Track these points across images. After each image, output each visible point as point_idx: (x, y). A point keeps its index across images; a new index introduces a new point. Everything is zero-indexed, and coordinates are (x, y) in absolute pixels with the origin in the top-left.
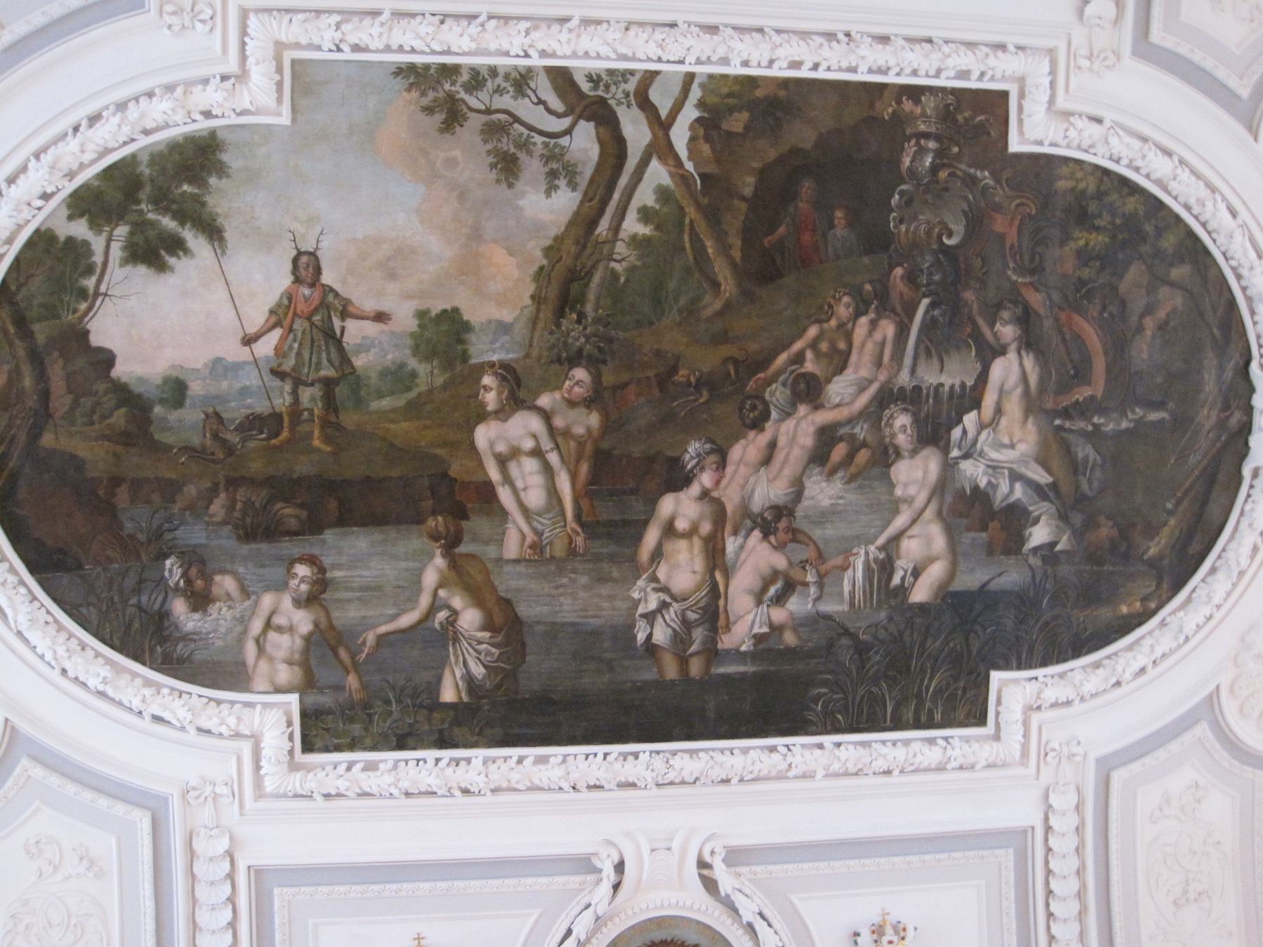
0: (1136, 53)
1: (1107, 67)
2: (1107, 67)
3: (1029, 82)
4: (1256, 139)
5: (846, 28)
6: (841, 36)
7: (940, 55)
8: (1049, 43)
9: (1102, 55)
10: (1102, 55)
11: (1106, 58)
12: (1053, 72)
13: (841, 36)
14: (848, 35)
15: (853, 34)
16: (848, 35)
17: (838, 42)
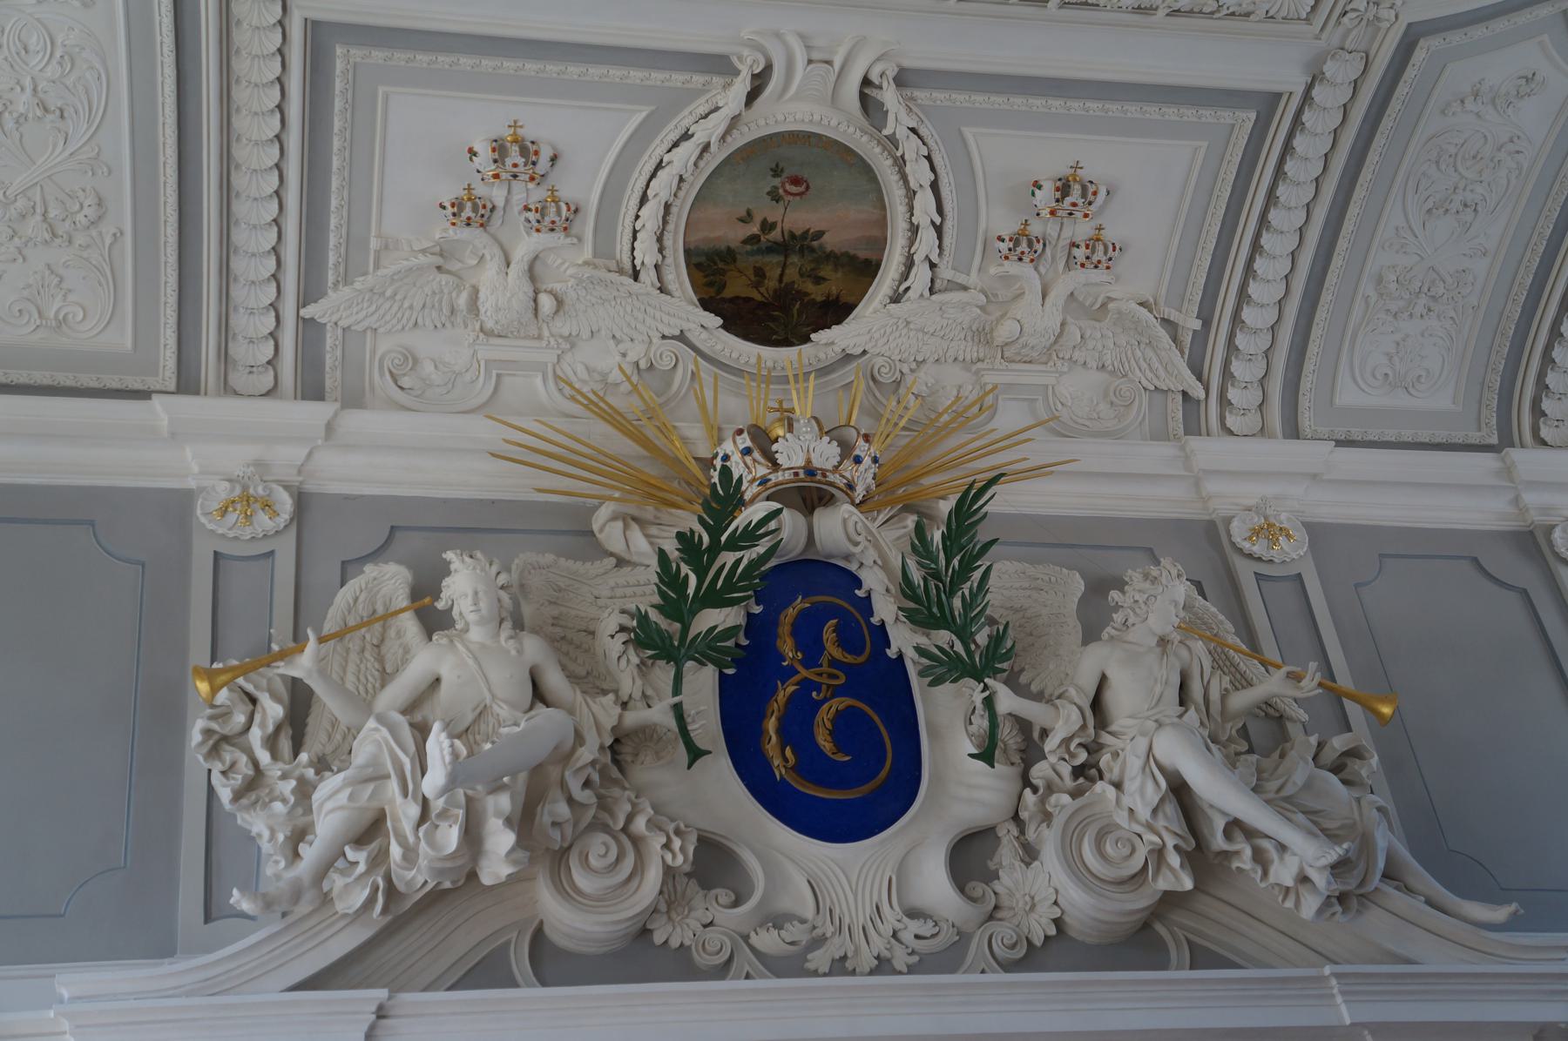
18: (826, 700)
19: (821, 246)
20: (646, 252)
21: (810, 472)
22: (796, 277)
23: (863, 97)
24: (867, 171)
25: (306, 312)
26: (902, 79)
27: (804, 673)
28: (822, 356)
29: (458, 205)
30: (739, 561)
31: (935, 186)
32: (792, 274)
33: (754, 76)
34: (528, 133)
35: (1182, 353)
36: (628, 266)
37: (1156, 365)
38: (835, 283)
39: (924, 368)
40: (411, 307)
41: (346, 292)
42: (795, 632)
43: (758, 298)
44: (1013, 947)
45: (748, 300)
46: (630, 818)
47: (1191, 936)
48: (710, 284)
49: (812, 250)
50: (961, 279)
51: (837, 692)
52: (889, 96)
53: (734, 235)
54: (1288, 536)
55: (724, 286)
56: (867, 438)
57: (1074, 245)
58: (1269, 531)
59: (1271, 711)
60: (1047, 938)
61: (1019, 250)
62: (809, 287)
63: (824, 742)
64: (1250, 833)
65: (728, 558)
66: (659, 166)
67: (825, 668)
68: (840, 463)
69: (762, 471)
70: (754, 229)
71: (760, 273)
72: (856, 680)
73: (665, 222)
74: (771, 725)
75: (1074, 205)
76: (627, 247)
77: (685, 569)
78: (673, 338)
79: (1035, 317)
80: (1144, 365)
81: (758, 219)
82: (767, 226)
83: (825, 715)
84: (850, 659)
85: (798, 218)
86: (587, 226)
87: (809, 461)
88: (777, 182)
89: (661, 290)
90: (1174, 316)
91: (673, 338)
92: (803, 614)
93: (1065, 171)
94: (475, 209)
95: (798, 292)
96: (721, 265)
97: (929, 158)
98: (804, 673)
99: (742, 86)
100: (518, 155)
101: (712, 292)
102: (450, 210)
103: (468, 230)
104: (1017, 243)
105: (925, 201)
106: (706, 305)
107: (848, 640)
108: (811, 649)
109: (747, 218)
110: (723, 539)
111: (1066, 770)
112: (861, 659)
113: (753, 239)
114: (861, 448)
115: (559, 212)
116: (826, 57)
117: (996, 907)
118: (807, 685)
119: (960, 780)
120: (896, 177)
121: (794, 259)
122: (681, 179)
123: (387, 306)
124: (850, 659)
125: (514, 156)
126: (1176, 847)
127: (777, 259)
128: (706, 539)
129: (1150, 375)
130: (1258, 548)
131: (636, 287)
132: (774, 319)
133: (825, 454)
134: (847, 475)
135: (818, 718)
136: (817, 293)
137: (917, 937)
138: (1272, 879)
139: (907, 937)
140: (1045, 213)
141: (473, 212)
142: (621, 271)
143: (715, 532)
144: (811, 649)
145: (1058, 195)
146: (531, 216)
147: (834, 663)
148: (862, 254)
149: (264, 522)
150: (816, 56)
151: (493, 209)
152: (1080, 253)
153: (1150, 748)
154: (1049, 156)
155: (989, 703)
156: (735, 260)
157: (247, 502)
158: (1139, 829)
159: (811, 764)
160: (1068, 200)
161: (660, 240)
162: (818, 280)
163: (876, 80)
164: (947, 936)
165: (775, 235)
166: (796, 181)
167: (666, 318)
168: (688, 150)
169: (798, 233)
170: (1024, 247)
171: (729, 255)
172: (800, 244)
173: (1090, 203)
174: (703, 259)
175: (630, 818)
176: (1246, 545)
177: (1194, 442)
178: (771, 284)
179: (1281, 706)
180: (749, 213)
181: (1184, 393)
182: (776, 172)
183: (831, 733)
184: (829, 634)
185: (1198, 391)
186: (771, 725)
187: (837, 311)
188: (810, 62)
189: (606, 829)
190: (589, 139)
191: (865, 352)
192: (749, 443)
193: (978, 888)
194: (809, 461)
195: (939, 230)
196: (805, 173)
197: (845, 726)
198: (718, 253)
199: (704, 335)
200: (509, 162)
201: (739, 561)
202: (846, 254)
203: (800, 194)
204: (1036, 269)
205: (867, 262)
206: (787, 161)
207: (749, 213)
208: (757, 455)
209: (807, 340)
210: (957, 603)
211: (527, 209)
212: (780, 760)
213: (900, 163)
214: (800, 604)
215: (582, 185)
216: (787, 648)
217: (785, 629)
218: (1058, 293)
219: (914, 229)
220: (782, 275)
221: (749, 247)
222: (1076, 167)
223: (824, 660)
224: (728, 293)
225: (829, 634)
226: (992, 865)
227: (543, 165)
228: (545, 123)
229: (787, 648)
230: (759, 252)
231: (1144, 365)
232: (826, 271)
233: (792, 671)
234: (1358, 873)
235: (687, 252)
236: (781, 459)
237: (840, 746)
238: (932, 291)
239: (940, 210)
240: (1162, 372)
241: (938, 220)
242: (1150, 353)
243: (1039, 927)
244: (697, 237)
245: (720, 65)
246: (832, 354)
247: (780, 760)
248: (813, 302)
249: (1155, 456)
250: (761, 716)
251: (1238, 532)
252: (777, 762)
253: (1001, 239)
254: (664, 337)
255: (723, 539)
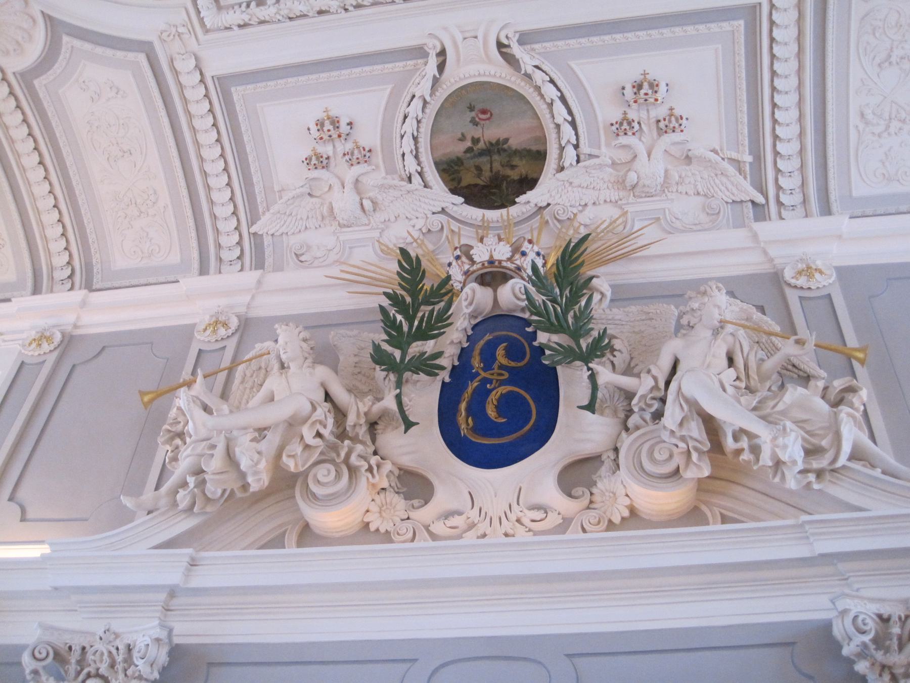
0: (150, 44)
1: (165, 31)
2: (165, 31)
3: (215, 9)
4: (42, 12)
5: (348, 14)
6: (351, 8)
7: (282, 13)
8: (211, 36)
9: (172, 37)
10: (172, 37)
11: (169, 36)
12: (201, 21)
13: (351, 8)
14: (346, 10)
15: (343, 11)
16: (346, 10)
17: (352, 5)
18: (493, 389)
19: (509, 147)
20: (411, 165)
21: (491, 262)
22: (500, 168)
23: (501, 53)
24: (522, 98)
25: (252, 230)
26: (525, 39)
27: (483, 374)
28: (524, 210)
29: (308, 160)
30: (432, 311)
31: (563, 99)
32: (497, 166)
33: (438, 55)
34: (333, 113)
35: (745, 178)
36: (405, 177)
37: (730, 187)
38: (523, 168)
39: (588, 209)
40: (301, 219)
41: (268, 215)
42: (481, 353)
43: (481, 183)
44: (599, 523)
45: (476, 185)
46: (348, 455)
47: (723, 511)
48: (453, 180)
49: (505, 150)
50: (595, 152)
51: (502, 383)
52: (516, 50)
53: (458, 149)
54: (821, 272)
55: (460, 181)
56: (530, 242)
57: (659, 121)
58: (808, 271)
59: (801, 373)
60: (623, 519)
61: (623, 128)
62: (509, 172)
63: (491, 412)
64: (751, 436)
65: (425, 309)
66: (405, 117)
67: (496, 370)
68: (512, 256)
69: (466, 267)
70: (469, 144)
71: (479, 169)
72: (515, 376)
73: (417, 149)
74: (463, 406)
75: (646, 94)
76: (401, 166)
77: (399, 317)
78: (439, 213)
79: (651, 170)
80: (723, 188)
81: (469, 137)
82: (475, 141)
83: (494, 397)
84: (513, 364)
85: (491, 133)
86: (378, 158)
87: (491, 256)
88: (473, 114)
89: (425, 186)
90: (734, 155)
91: (439, 213)
92: (488, 343)
93: (639, 78)
94: (317, 159)
95: (503, 176)
96: (456, 168)
97: (552, 81)
98: (483, 374)
99: (433, 62)
100: (331, 127)
101: (455, 184)
102: (306, 162)
103: (316, 171)
104: (621, 124)
105: (559, 107)
106: (454, 191)
107: (514, 351)
108: (488, 358)
109: (463, 138)
110: (420, 297)
111: (648, 417)
112: (519, 364)
113: (469, 150)
114: (526, 247)
115: (360, 152)
116: (473, 34)
117: (591, 502)
118: (485, 381)
119: (578, 429)
120: (538, 98)
121: (496, 157)
122: (419, 122)
123: (289, 220)
124: (513, 364)
125: (328, 126)
126: (696, 449)
127: (485, 159)
128: (408, 299)
129: (728, 193)
130: (802, 281)
131: (410, 187)
132: (494, 194)
133: (502, 252)
134: (518, 262)
135: (489, 399)
136: (514, 175)
137: (533, 521)
138: (761, 463)
139: (526, 521)
140: (631, 103)
141: (319, 162)
142: (402, 180)
143: (414, 293)
144: (488, 358)
145: (635, 90)
146: (347, 157)
147: (501, 367)
148: (534, 148)
149: (222, 332)
150: (467, 35)
151: (328, 158)
152: (662, 125)
153: (680, 388)
154: (629, 69)
155: (593, 377)
156: (462, 164)
157: (217, 323)
158: (674, 441)
159: (483, 426)
160: (642, 92)
161: (416, 157)
162: (513, 167)
163: (505, 42)
164: (553, 520)
165: (481, 145)
166: (484, 112)
167: (431, 202)
168: (417, 104)
169: (494, 142)
170: (625, 126)
171: (458, 162)
172: (496, 148)
173: (656, 92)
174: (445, 166)
175: (348, 455)
176: (793, 281)
177: (758, 227)
178: (487, 174)
179: (808, 370)
180: (463, 135)
181: (753, 202)
182: (471, 108)
183: (496, 407)
184: (500, 352)
185: (760, 199)
186: (463, 406)
187: (528, 183)
188: (465, 39)
189: (332, 461)
190: (364, 107)
191: (549, 205)
192: (459, 253)
193: (578, 491)
194: (491, 256)
195: (573, 124)
196: (487, 106)
197: (507, 404)
198: (452, 161)
199: (455, 208)
200: (325, 129)
201: (433, 310)
202: (525, 150)
203: (488, 119)
204: (640, 140)
205: (538, 152)
206: (477, 101)
207: (463, 135)
208: (464, 259)
209: (514, 203)
210: (570, 320)
211: (344, 155)
212: (464, 423)
213: (538, 89)
214: (488, 337)
215: (368, 135)
216: (476, 363)
217: (477, 352)
218: (658, 153)
219: (558, 126)
220: (491, 168)
221: (468, 155)
222: (645, 74)
223: (495, 366)
224: (464, 183)
225: (500, 352)
226: (594, 477)
227: (344, 128)
228: (343, 106)
229: (476, 363)
230: (475, 156)
231: (723, 188)
232: (516, 161)
233: (477, 374)
234: (829, 456)
235: (437, 164)
236: (476, 258)
237: (500, 415)
238: (578, 161)
239: (570, 112)
240: (735, 191)
241: (570, 119)
242: (724, 180)
243: (619, 512)
244: (439, 153)
245: (420, 52)
246: (530, 208)
247: (464, 423)
248: (514, 181)
249: (736, 237)
250: (458, 402)
251: (788, 275)
252: (463, 426)
253: (612, 125)
254: (434, 213)
255: (420, 297)
